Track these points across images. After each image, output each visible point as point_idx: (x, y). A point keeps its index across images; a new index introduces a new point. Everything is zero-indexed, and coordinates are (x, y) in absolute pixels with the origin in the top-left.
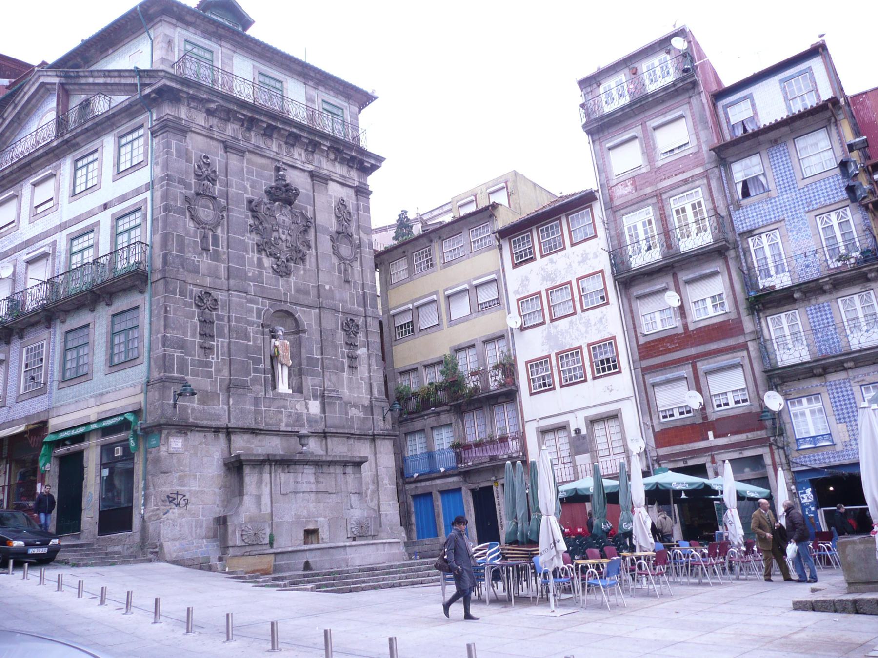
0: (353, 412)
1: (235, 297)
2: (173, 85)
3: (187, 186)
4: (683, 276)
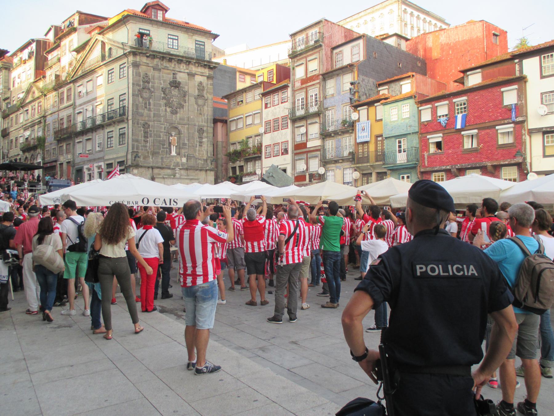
0: (200, 161)
2: (133, 50)
3: (139, 86)
4: (309, 122)
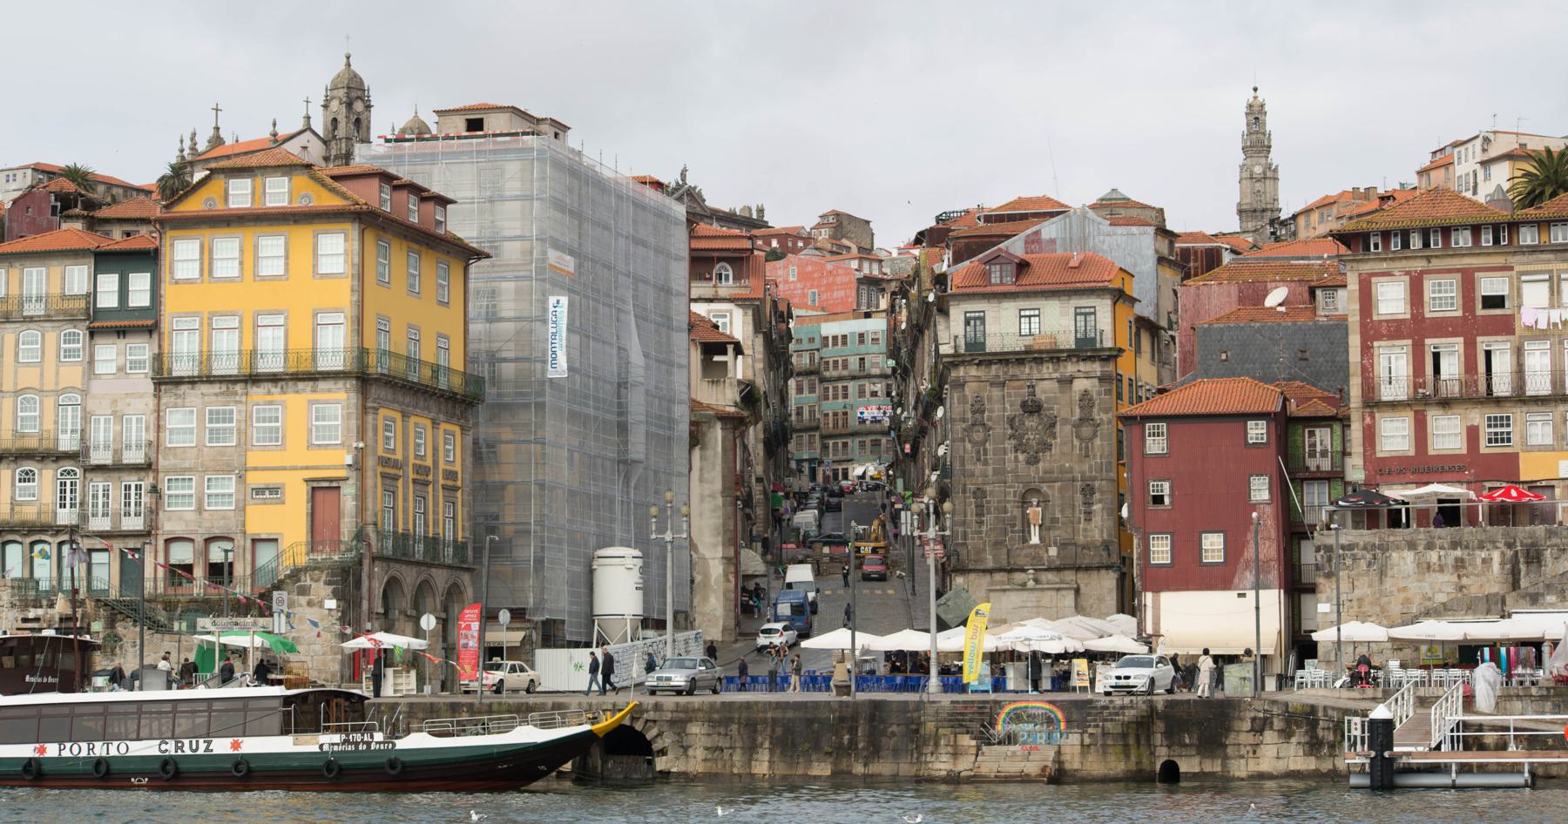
1: (997, 488)
3: (964, 420)
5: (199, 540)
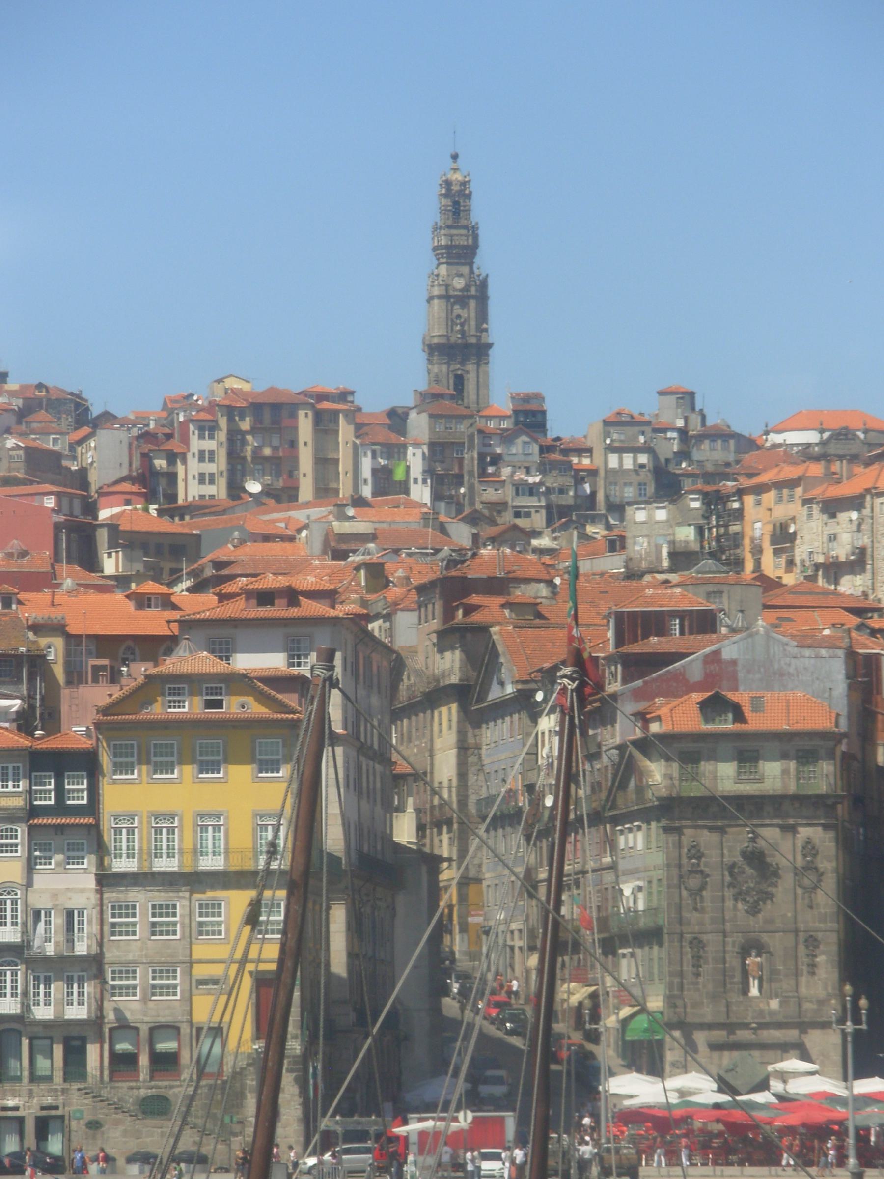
5: (144, 1030)
